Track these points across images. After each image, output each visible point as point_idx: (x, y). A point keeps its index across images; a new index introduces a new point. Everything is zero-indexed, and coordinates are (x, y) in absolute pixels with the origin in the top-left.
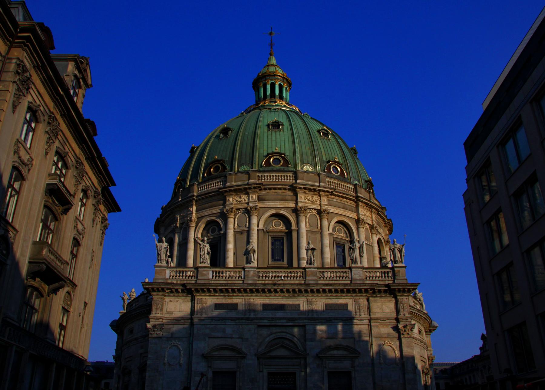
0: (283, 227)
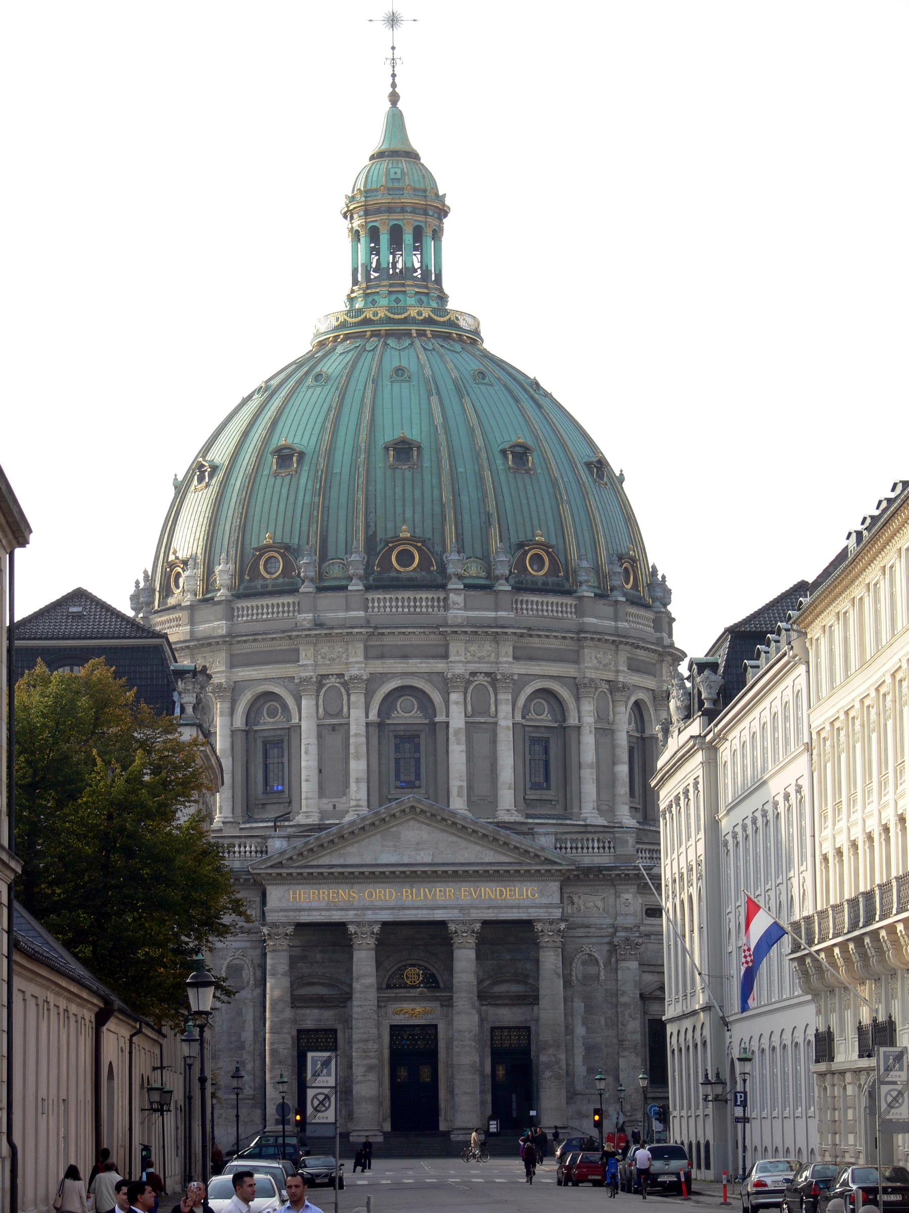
0: (419, 712)
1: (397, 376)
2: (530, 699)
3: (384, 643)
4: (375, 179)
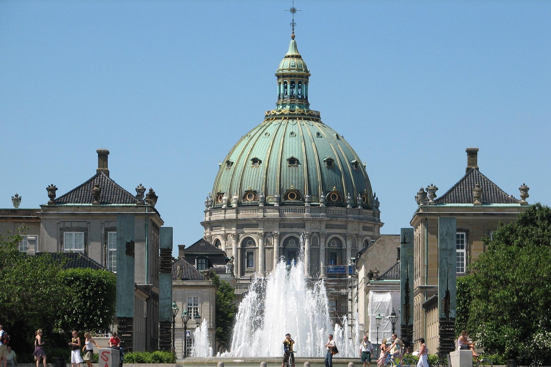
1: (291, 134)
2: (331, 240)
3: (285, 223)
4: (286, 65)
